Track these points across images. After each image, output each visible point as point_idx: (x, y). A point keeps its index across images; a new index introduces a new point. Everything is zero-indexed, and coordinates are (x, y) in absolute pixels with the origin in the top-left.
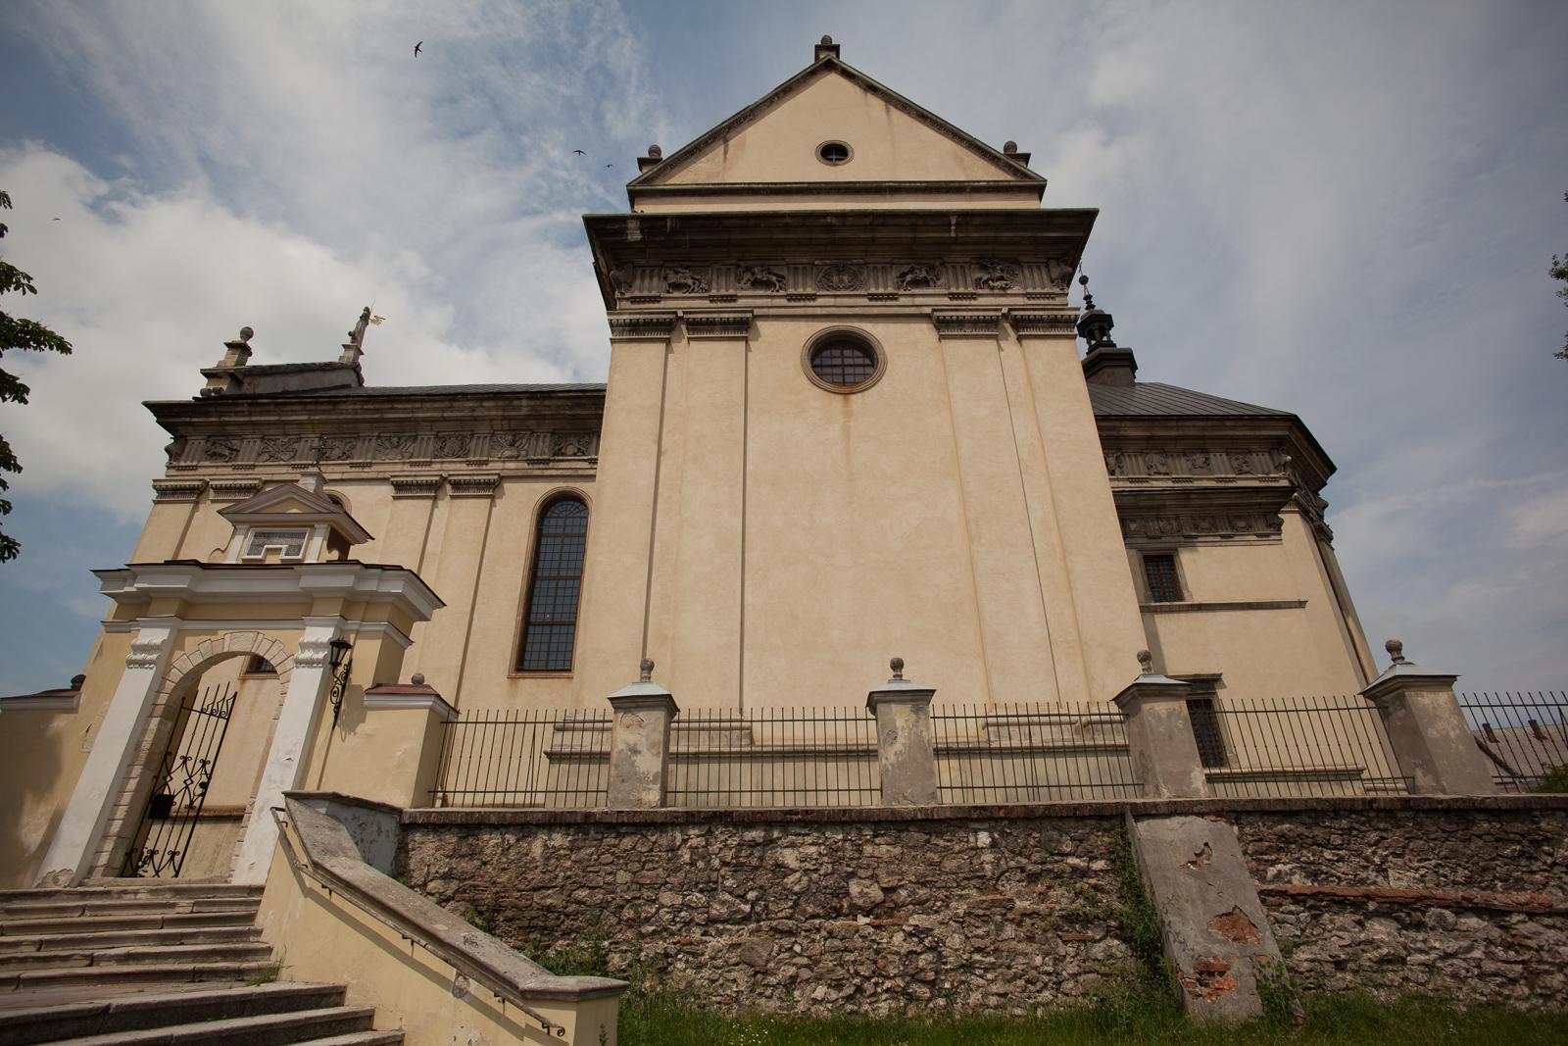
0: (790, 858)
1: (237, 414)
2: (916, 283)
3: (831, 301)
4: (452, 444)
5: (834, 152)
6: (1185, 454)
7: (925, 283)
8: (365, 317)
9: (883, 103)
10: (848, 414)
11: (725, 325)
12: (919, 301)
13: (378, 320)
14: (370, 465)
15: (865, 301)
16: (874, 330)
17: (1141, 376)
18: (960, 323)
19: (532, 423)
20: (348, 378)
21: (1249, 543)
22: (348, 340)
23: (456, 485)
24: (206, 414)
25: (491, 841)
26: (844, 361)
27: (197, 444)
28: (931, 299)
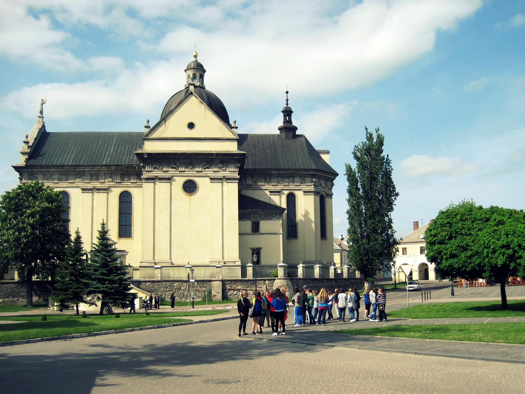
1: (37, 169)
2: (206, 168)
3: (188, 172)
4: (94, 177)
5: (191, 126)
6: (288, 177)
7: (208, 168)
9: (204, 107)
10: (190, 201)
11: (166, 179)
12: (207, 172)
14: (74, 183)
15: (195, 172)
16: (196, 180)
17: (298, 132)
18: (214, 179)
19: (115, 172)
20: (43, 130)
23: (98, 189)
24: (28, 169)
26: (190, 187)
27: (26, 175)
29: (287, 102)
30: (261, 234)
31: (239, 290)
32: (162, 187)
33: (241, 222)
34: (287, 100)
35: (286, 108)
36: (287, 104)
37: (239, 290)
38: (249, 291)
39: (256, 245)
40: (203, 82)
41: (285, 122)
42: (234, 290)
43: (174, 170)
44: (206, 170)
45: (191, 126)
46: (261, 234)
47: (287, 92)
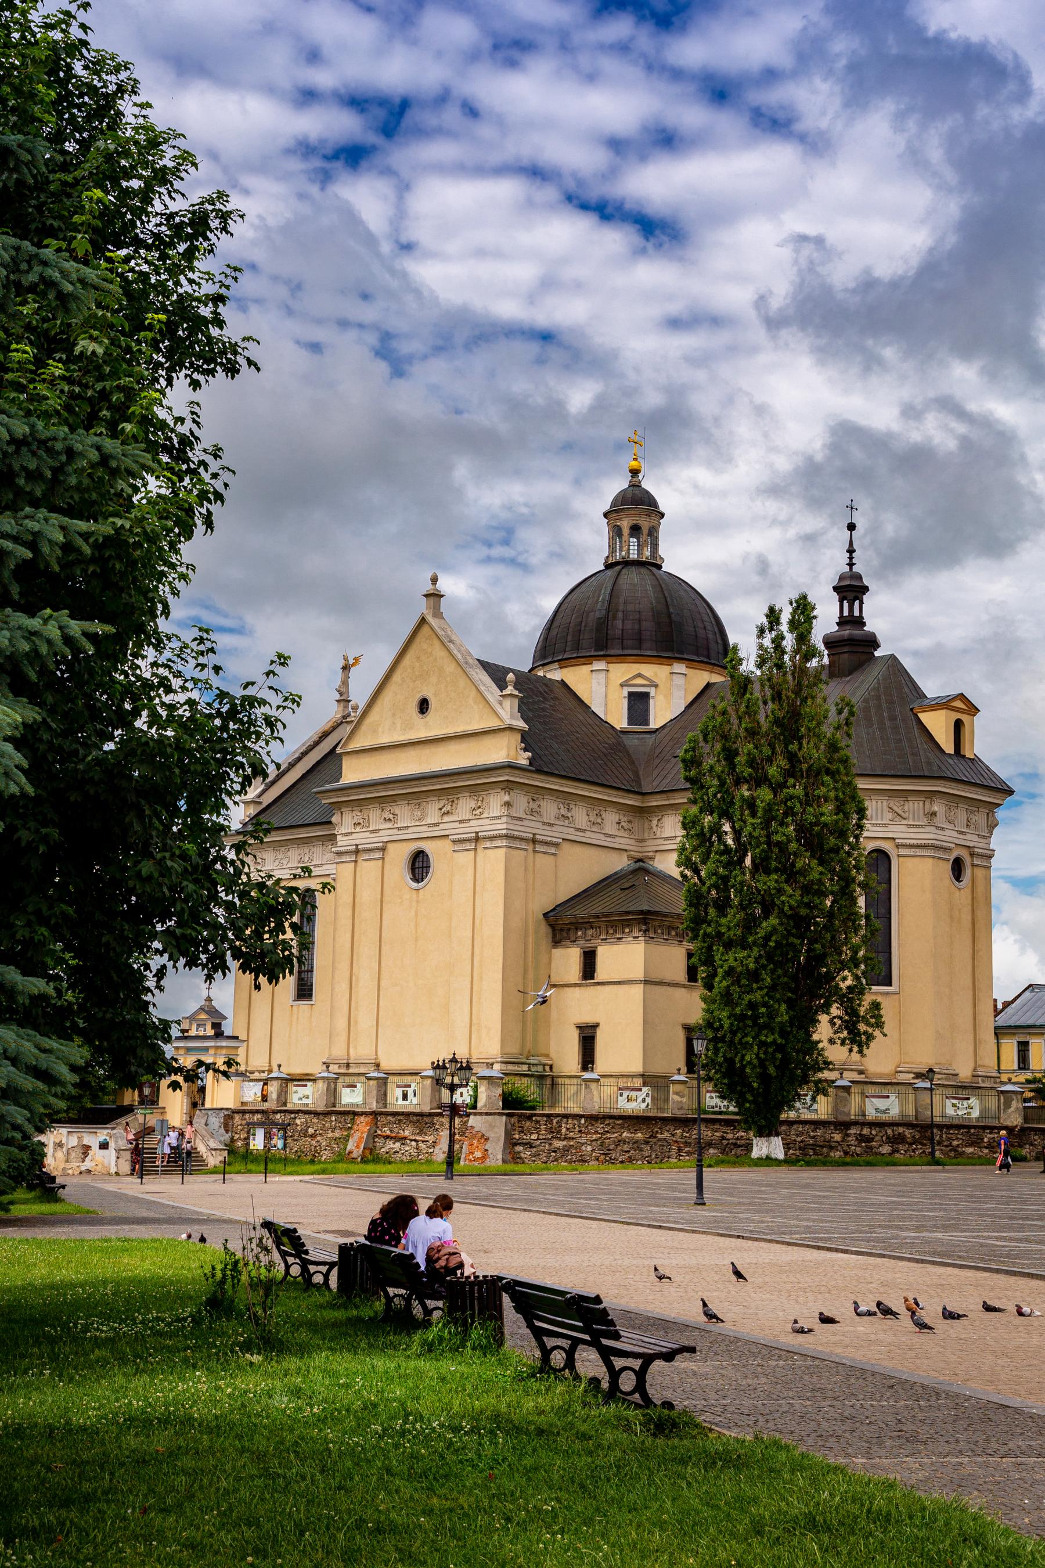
0: (298, 1121)
5: (424, 706)
8: (346, 668)
13: (357, 660)
21: (629, 943)
22: (338, 697)
25: (247, 1116)
28: (451, 827)
29: (851, 558)
30: (599, 984)
31: (403, 1140)
32: (369, 869)
33: (557, 953)
34: (851, 551)
35: (842, 578)
36: (851, 565)
37: (403, 1140)
38: (421, 1144)
39: (588, 1019)
40: (655, 546)
41: (842, 622)
42: (396, 1139)
43: (389, 825)
44: (446, 819)
45: (424, 706)
46: (599, 984)
47: (851, 527)
